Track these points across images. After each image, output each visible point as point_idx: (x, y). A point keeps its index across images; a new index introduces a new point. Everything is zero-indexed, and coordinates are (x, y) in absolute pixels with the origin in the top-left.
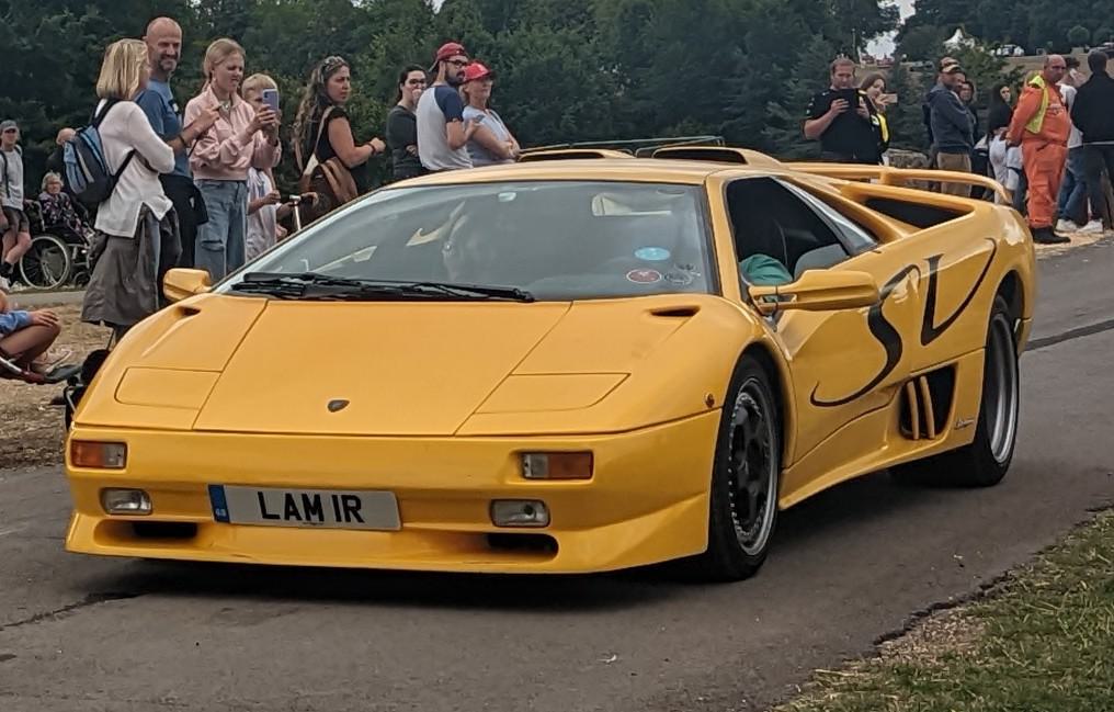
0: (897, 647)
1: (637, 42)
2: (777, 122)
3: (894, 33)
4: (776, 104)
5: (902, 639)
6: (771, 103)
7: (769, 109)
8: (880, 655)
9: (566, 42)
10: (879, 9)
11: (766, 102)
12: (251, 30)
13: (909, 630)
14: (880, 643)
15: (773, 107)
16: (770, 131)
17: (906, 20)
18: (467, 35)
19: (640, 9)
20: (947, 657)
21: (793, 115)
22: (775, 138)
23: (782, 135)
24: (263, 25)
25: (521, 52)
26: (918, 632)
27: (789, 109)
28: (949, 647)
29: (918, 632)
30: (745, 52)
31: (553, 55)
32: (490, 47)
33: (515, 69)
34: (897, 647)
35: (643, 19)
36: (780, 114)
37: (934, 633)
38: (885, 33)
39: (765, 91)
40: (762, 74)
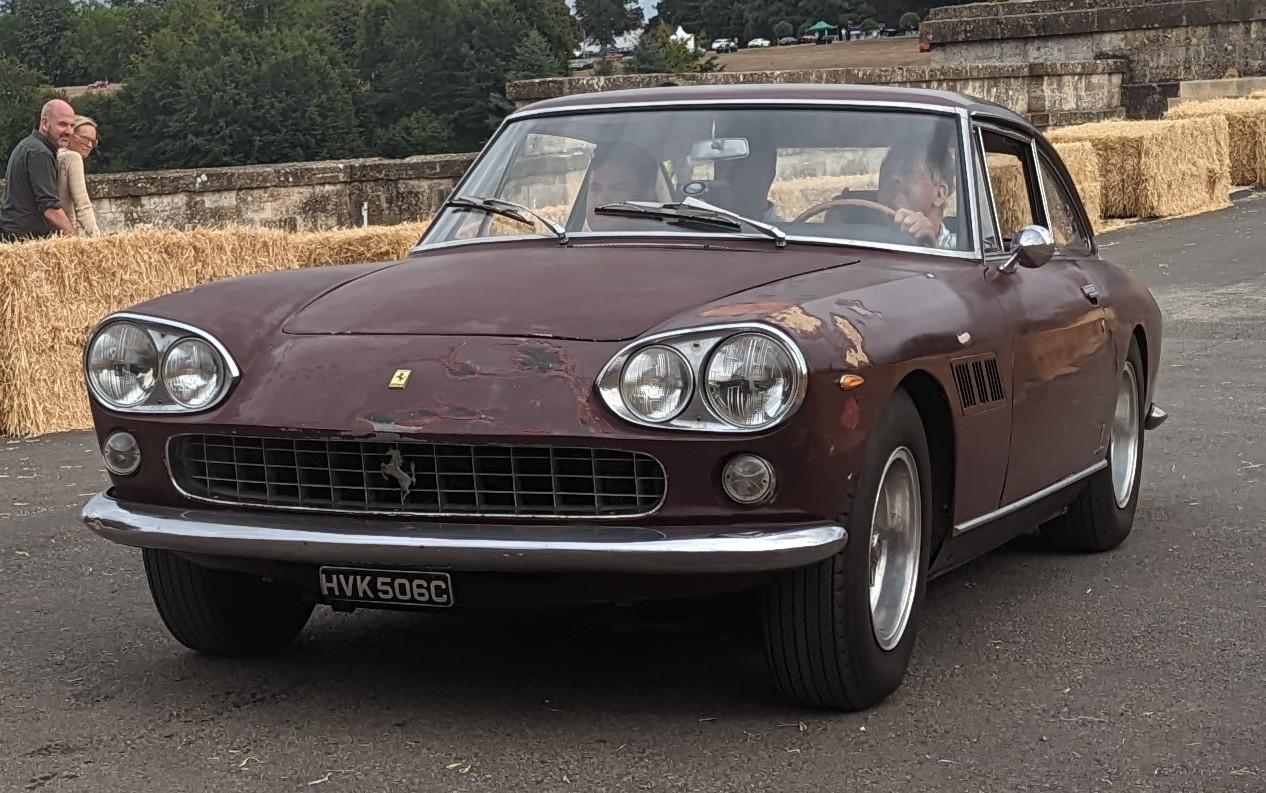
1: (379, 40)
3: (640, 31)
4: (498, 95)
6: (492, 94)
7: (493, 100)
9: (312, 40)
10: (625, 9)
12: (69, 33)
15: (495, 98)
17: (650, 20)
18: (223, 35)
19: (381, 11)
24: (78, 28)
25: (270, 50)
30: (472, 48)
31: (299, 53)
32: (245, 45)
33: (264, 67)
35: (383, 20)
36: (500, 104)
38: (632, 32)
39: (489, 84)
40: (487, 67)
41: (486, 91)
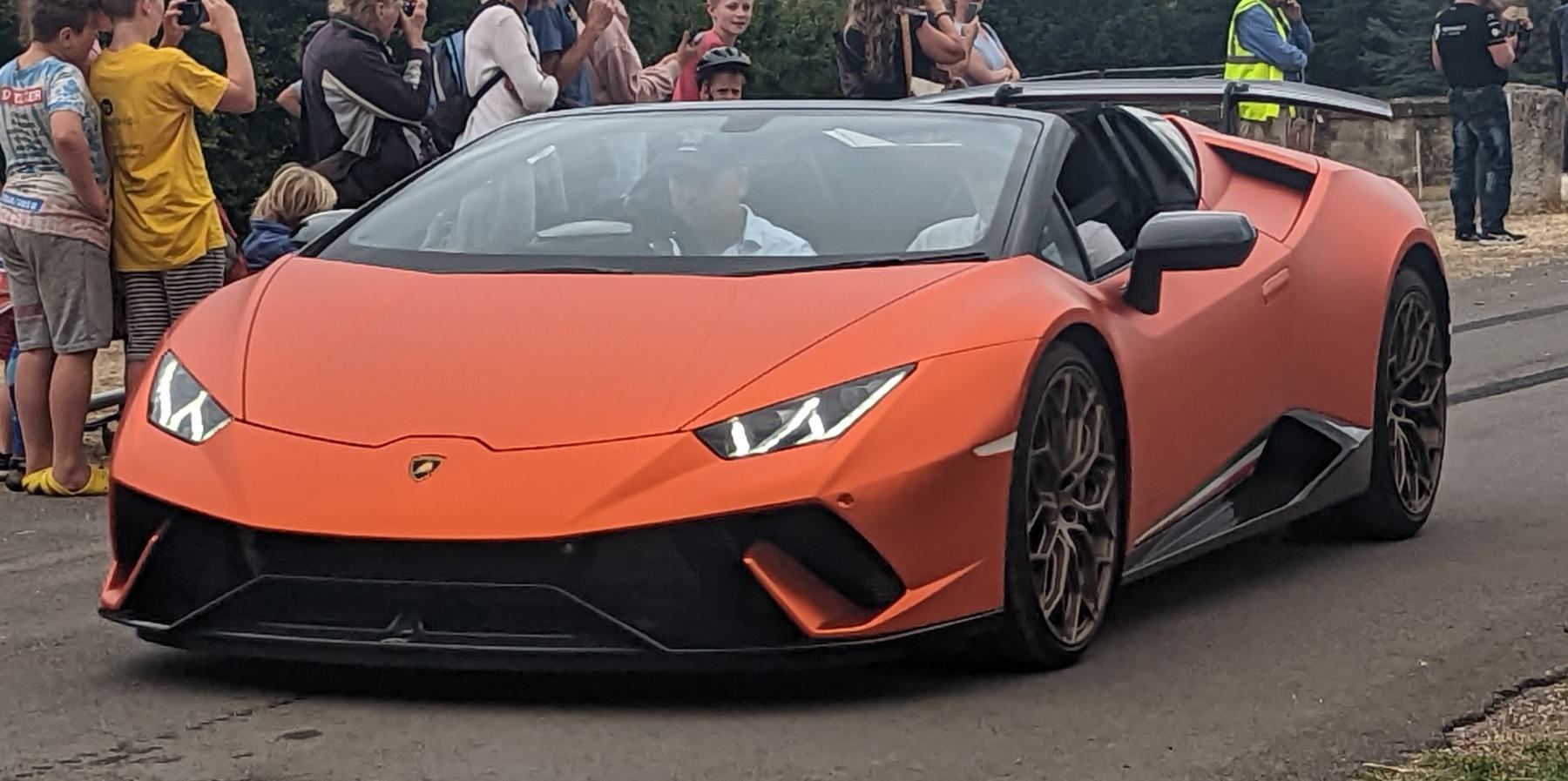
0: (1474, 735)
2: (1379, 45)
4: (1378, 21)
5: (1479, 725)
8: (1449, 745)
11: (1364, 19)
13: (1490, 713)
14: (1451, 729)
16: (1369, 57)
20: (1539, 748)
21: (1401, 36)
22: (1375, 65)
23: (1387, 61)
26: (1503, 717)
27: (1395, 28)
28: (1540, 736)
29: (1503, 717)
34: (1474, 735)
36: (1383, 34)
37: (1523, 718)
41: (1362, 16)
